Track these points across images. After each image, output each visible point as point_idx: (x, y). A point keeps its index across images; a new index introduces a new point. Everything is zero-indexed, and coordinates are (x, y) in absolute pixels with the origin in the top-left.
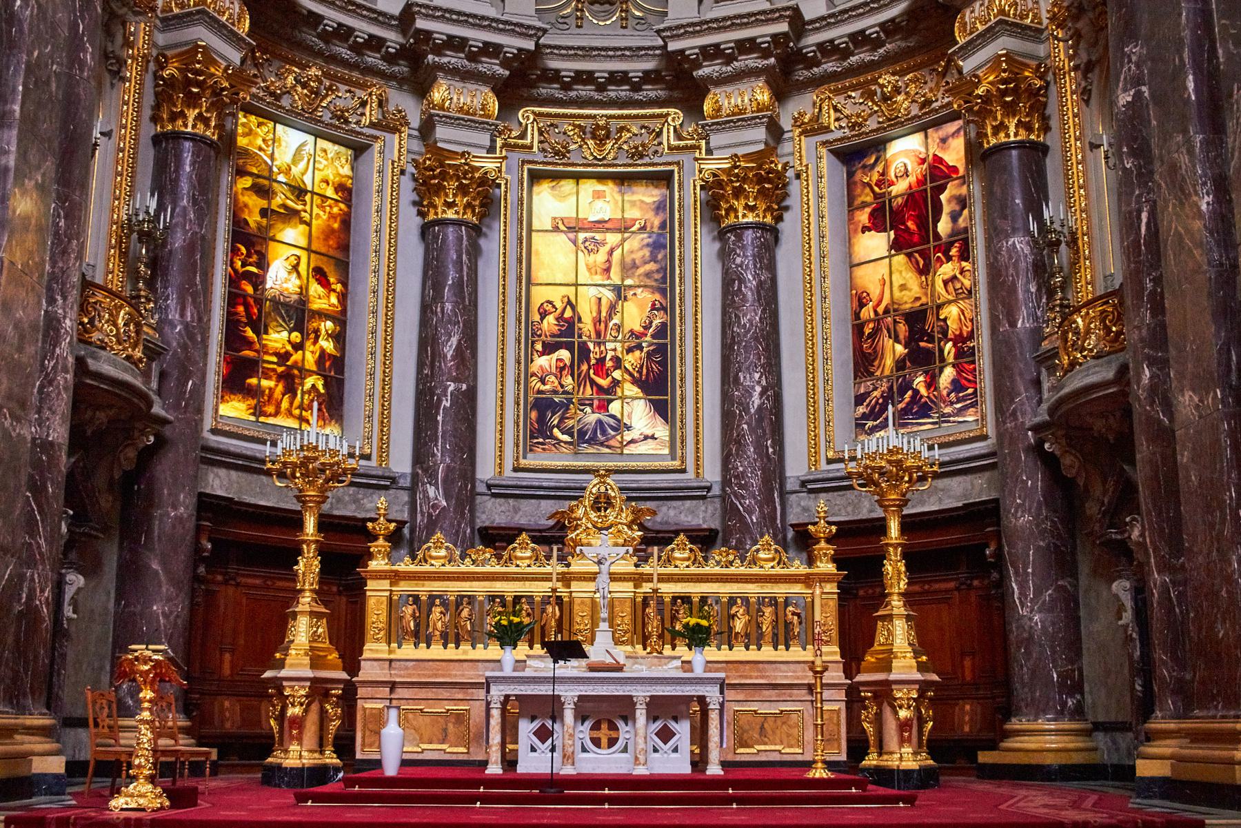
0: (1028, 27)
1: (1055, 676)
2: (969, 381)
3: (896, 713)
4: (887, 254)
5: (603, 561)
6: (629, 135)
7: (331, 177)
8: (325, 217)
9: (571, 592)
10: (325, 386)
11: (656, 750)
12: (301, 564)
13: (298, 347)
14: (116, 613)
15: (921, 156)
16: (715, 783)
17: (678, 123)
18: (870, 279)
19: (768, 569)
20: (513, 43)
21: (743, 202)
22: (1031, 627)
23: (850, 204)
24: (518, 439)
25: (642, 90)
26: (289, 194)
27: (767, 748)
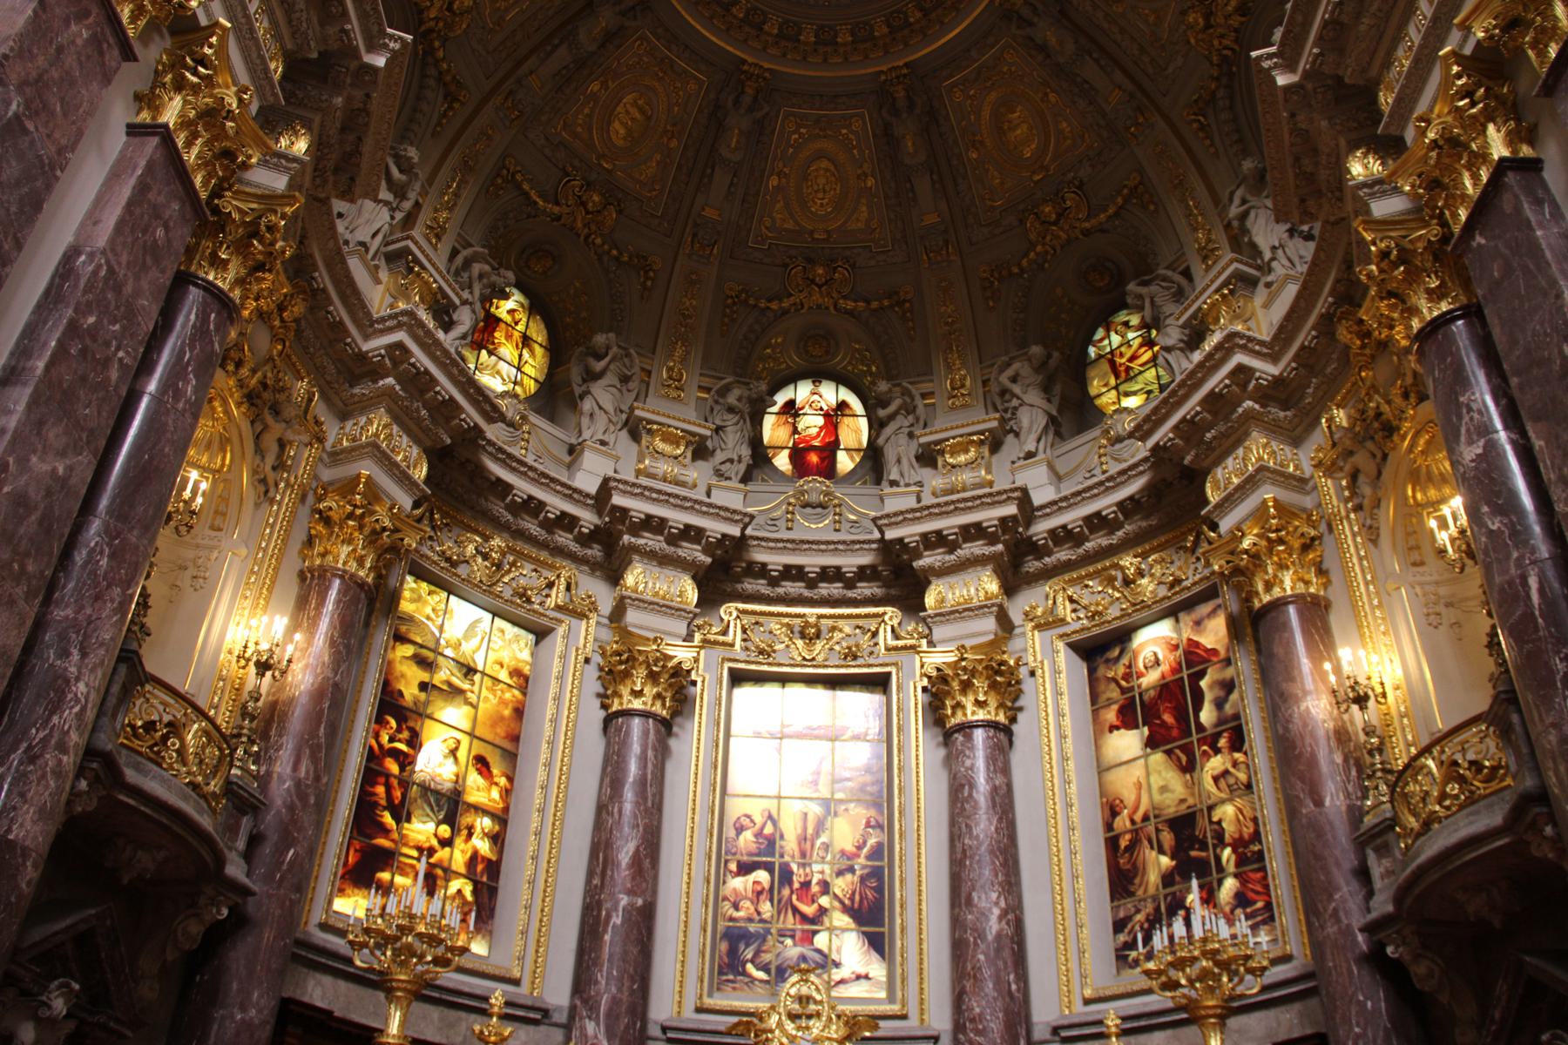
0: (1291, 476)
2: (1257, 893)
4: (1140, 753)
6: (841, 635)
7: (506, 661)
8: (495, 701)
10: (475, 892)
13: (446, 843)
17: (895, 622)
18: (1125, 783)
20: (716, 528)
21: (971, 698)
24: (703, 973)
25: (855, 587)
26: (455, 671)
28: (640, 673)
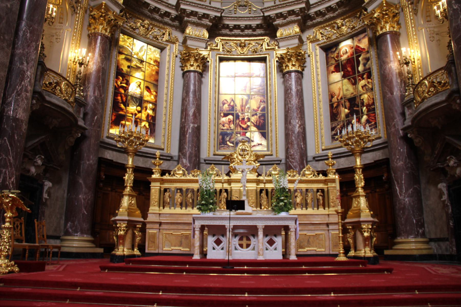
1: (415, 221)
2: (373, 120)
3: (362, 234)
5: (244, 171)
6: (252, 46)
7: (152, 58)
8: (150, 70)
9: (231, 187)
10: (149, 125)
11: (267, 249)
12: (126, 176)
13: (140, 112)
14: (67, 198)
15: (352, 46)
16: (293, 263)
17: (268, 41)
18: (336, 88)
19: (310, 177)
20: (213, 14)
21: (291, 63)
22: (404, 203)
23: (327, 64)
25: (256, 31)
26: (138, 62)
27: (311, 249)
28: (192, 60)
